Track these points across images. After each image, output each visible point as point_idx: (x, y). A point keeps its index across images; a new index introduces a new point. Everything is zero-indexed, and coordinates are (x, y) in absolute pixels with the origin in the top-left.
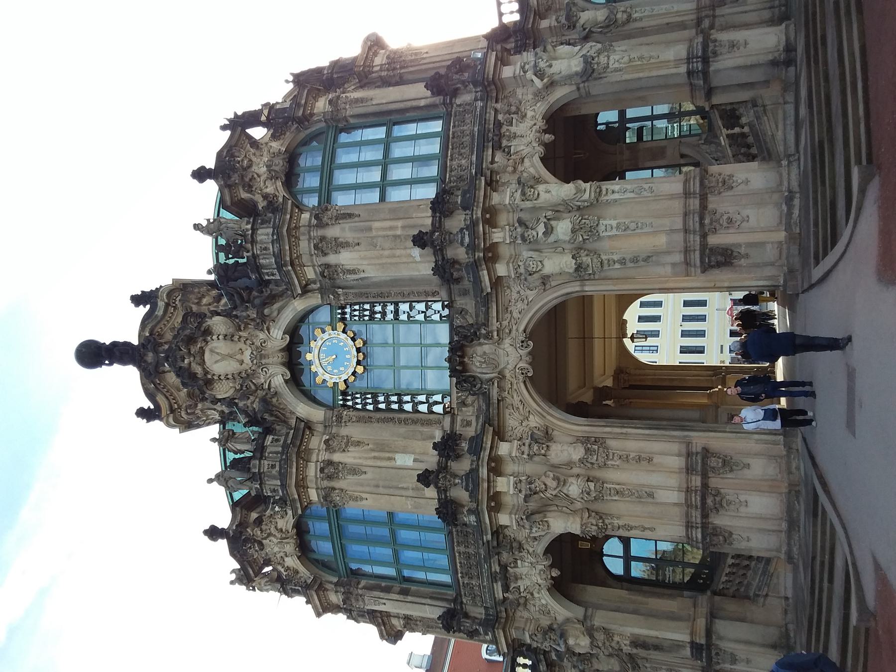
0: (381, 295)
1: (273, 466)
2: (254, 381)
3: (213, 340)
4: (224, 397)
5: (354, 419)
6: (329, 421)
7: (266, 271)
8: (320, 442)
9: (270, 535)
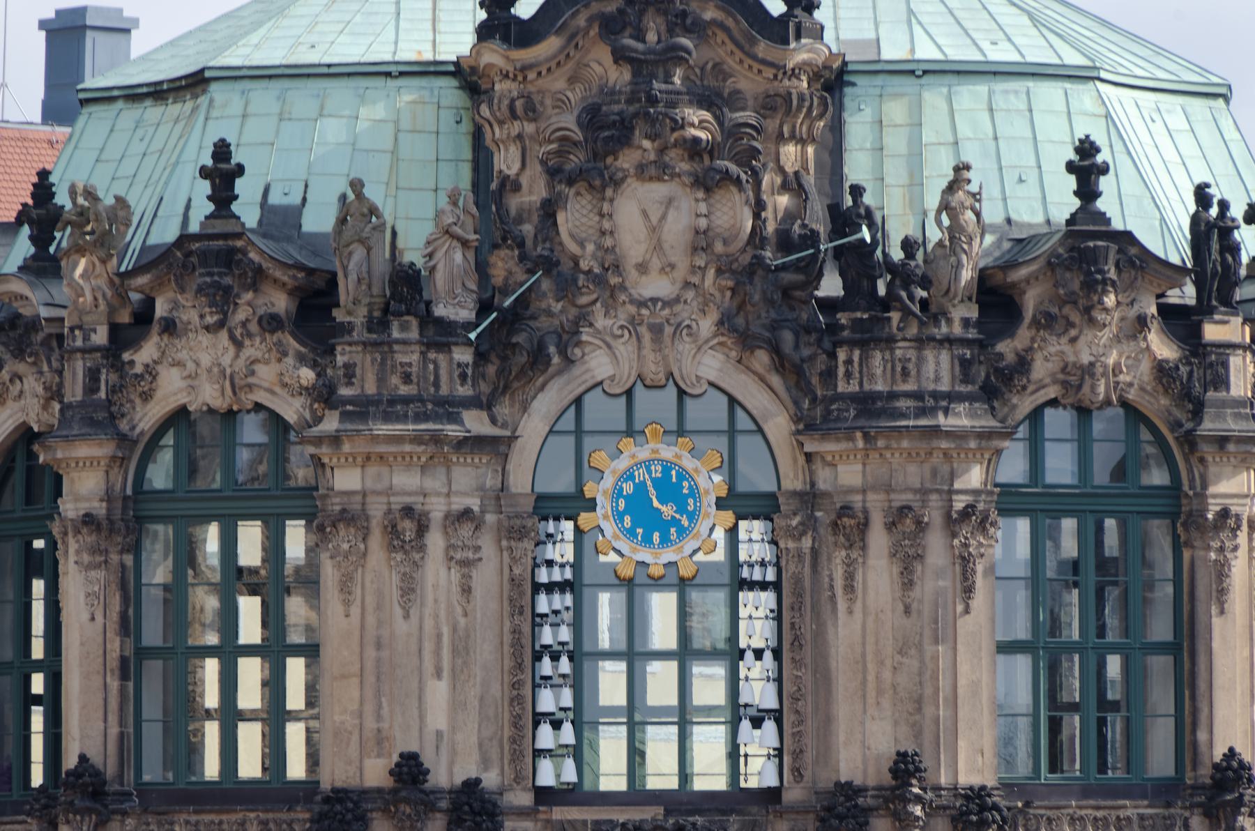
0: (797, 641)
1: (407, 378)
2: (598, 305)
3: (697, 200)
4: (563, 229)
5: (517, 571)
6: (511, 506)
7: (856, 358)
8: (465, 494)
9: (238, 345)
